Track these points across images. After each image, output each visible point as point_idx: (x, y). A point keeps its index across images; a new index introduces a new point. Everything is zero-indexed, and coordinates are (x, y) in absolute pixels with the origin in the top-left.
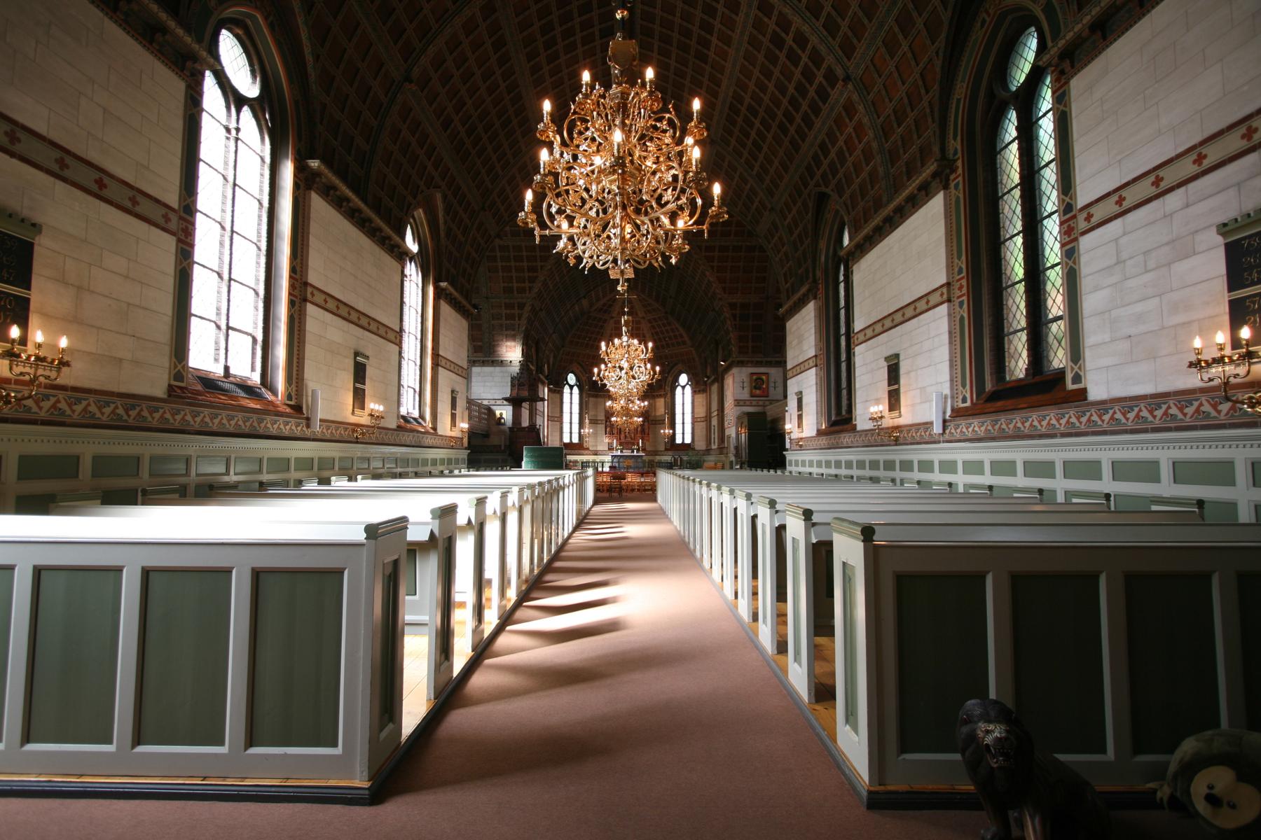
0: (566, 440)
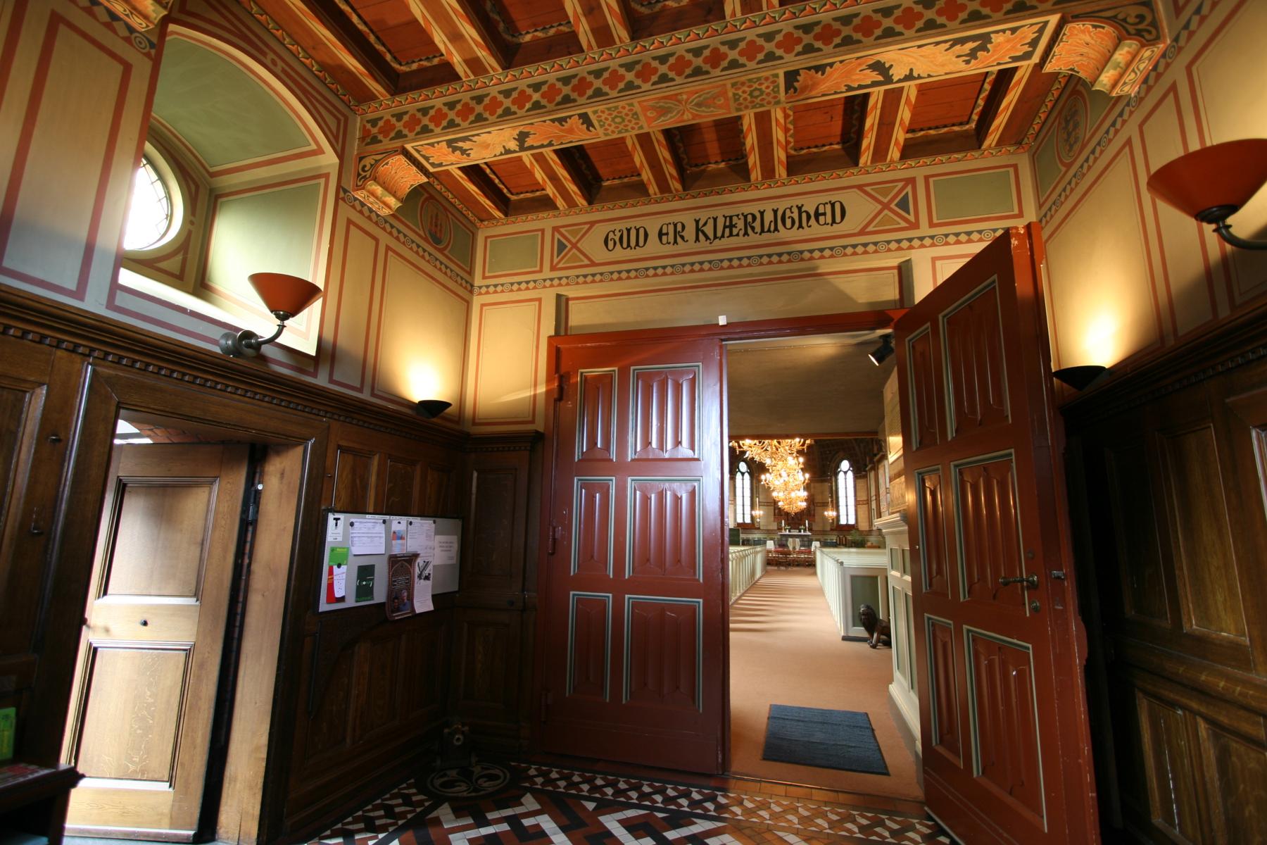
0: (740, 520)
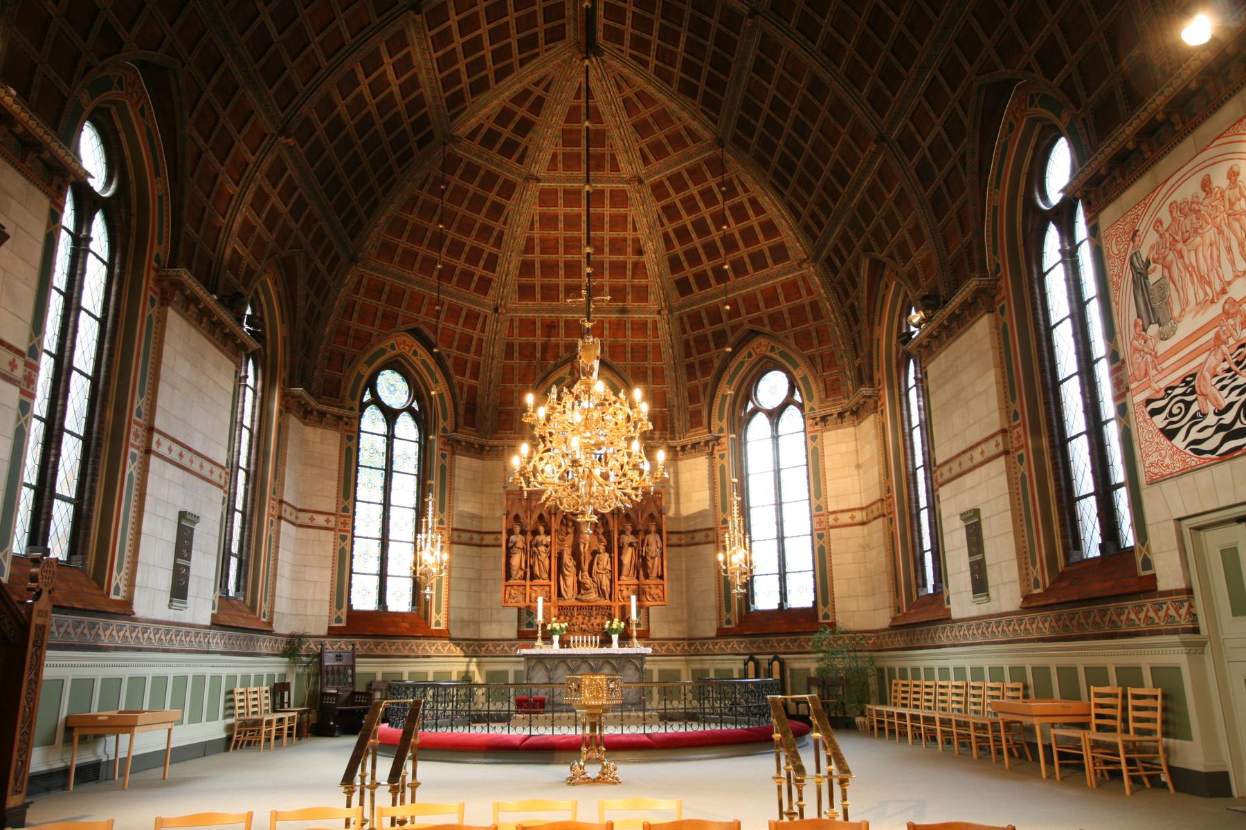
0: (363, 598)
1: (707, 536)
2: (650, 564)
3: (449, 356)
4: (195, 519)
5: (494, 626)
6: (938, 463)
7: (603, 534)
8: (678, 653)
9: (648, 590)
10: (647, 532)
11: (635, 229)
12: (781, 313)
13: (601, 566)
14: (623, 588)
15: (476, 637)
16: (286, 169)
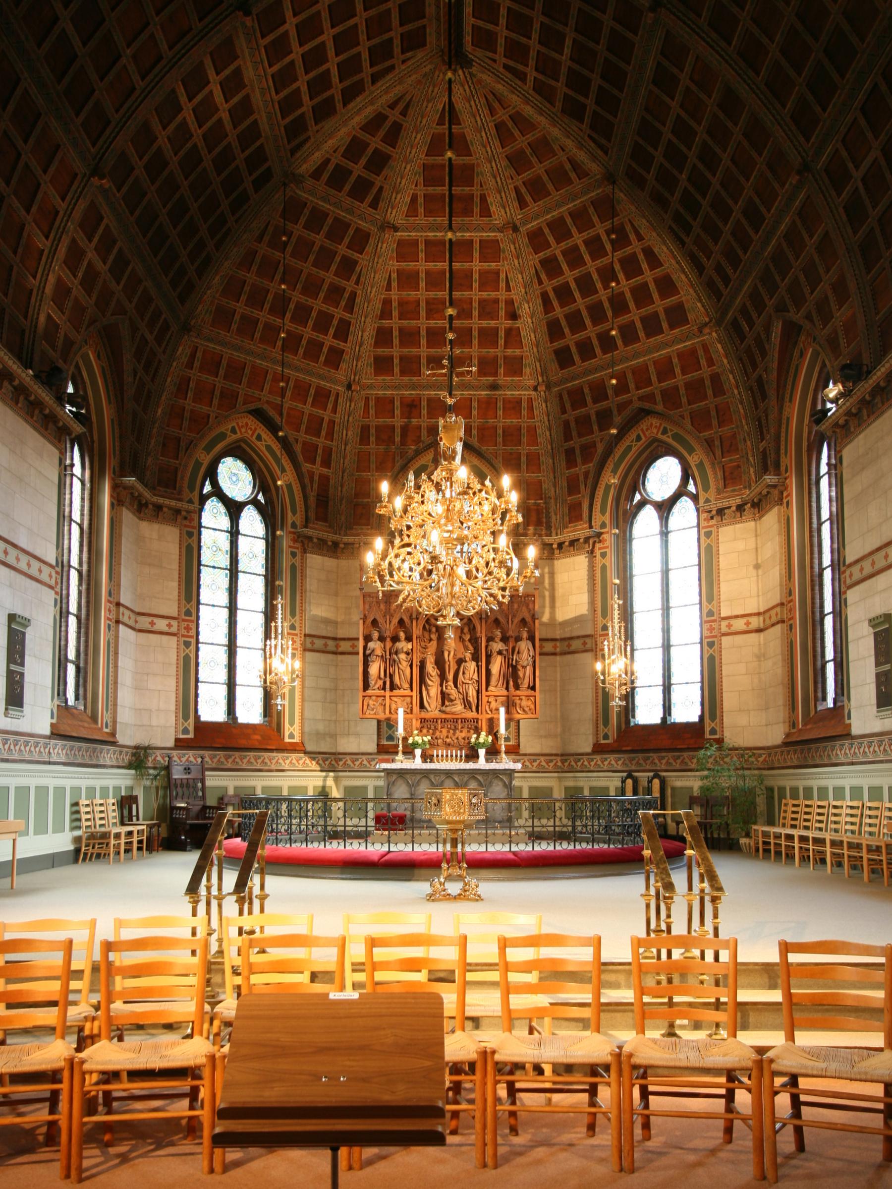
1: (585, 644)
2: (521, 674)
3: (297, 441)
4: (26, 622)
5: (352, 739)
6: (848, 562)
7: (470, 640)
8: (550, 769)
9: (518, 702)
10: (518, 639)
11: (508, 289)
12: (676, 388)
13: (467, 676)
14: (491, 699)
15: (333, 751)
16: (101, 219)
